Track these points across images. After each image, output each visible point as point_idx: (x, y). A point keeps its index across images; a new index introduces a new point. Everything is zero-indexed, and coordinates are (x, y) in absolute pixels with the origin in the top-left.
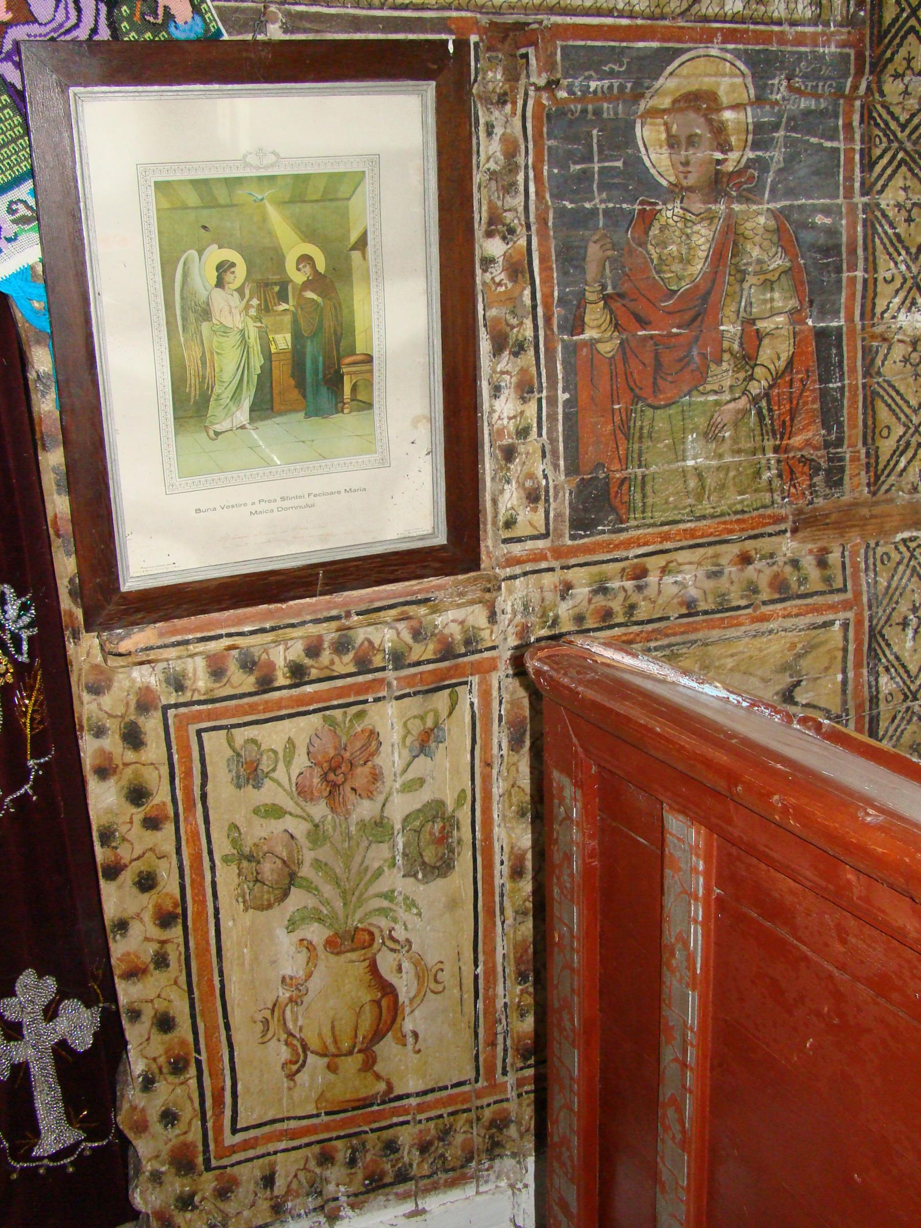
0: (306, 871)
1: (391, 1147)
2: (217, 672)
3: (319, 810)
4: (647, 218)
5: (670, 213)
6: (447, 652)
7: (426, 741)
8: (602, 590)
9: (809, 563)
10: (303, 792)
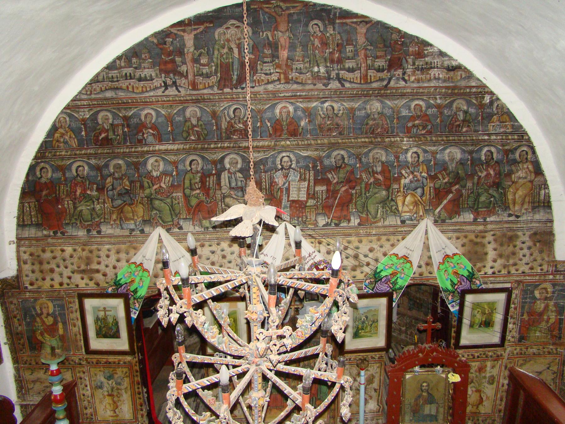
0: (474, 381)
1: (478, 420)
2: (468, 355)
3: (477, 374)
4: (535, 302)
5: (538, 302)
7: (493, 367)
8: (521, 350)
10: (476, 371)
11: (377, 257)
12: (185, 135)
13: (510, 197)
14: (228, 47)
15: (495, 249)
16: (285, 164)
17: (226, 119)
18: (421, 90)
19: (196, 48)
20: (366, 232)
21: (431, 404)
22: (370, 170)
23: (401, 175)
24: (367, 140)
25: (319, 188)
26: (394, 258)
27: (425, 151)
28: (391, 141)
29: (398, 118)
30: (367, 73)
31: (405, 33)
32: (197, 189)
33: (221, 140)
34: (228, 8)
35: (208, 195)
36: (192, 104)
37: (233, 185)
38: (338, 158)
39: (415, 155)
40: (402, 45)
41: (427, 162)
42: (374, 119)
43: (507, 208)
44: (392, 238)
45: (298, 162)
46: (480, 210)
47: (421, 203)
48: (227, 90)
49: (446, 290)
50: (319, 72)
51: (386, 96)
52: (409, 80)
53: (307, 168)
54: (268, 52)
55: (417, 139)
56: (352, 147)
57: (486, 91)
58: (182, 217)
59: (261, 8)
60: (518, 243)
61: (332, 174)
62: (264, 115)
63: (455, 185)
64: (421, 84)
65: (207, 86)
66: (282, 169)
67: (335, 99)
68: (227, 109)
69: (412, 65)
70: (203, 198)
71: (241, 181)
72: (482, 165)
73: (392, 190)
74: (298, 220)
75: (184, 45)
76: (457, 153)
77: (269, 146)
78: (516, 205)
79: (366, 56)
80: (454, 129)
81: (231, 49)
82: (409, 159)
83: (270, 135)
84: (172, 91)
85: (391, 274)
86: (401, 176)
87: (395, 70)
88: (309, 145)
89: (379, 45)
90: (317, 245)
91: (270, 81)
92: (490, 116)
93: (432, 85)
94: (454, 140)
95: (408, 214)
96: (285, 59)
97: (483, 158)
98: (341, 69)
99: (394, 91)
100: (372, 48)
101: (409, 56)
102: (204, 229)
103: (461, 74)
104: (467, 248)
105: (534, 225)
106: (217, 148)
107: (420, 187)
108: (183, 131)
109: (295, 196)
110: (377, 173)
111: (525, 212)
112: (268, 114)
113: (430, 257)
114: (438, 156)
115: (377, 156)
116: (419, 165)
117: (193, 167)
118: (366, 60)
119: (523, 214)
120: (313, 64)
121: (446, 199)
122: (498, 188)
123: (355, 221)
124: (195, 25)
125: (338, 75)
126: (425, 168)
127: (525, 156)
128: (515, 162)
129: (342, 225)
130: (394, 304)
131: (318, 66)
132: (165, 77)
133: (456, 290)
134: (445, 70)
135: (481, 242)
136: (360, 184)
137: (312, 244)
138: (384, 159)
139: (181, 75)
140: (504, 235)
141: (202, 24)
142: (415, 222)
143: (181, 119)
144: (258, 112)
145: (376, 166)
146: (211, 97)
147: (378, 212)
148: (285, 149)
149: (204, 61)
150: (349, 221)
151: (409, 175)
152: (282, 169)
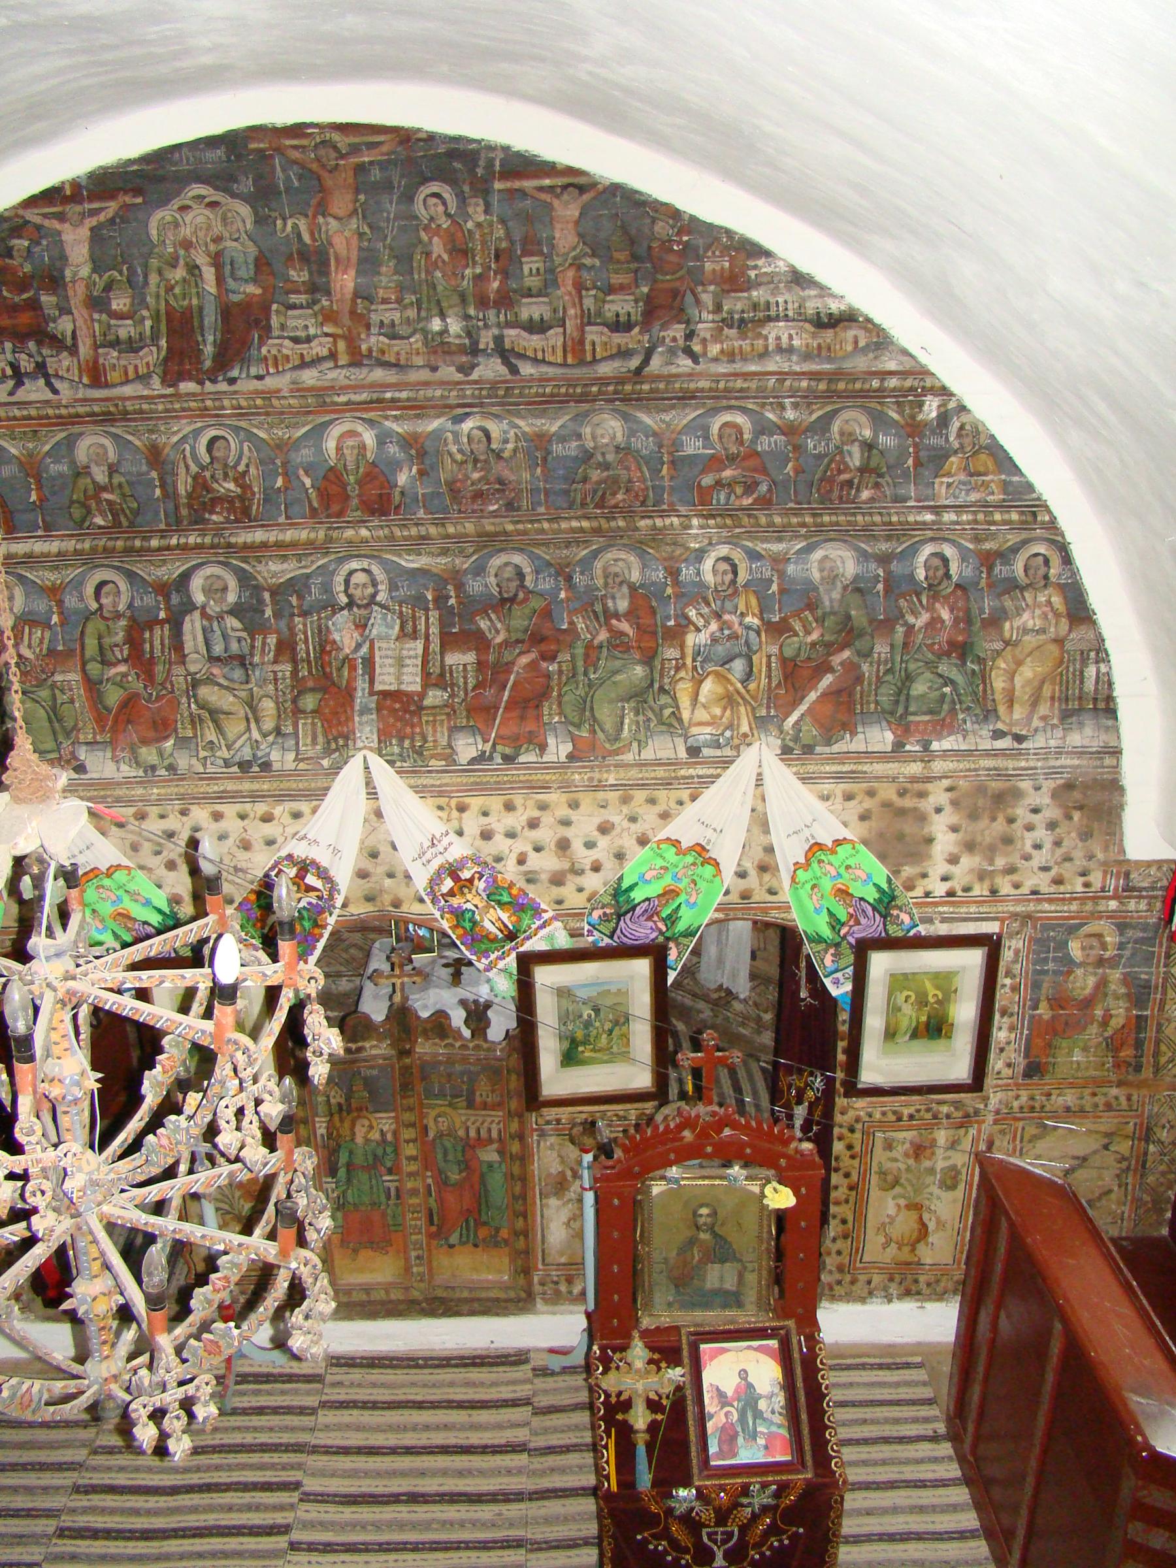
0: (902, 1181)
1: (916, 1281)
2: (884, 1114)
3: (911, 1162)
4: (1069, 973)
5: (1079, 972)
6: (967, 1116)
8: (1032, 1098)
9: (1123, 1100)
10: (906, 1155)
11: (622, 847)
12: (77, 512)
13: (999, 683)
14: (187, 264)
15: (954, 829)
16: (357, 593)
17: (187, 467)
18: (739, 384)
19: (98, 266)
20: (591, 779)
21: (723, 1261)
22: (598, 608)
23: (684, 622)
24: (585, 524)
25: (454, 659)
26: (670, 853)
27: (753, 556)
28: (654, 527)
29: (672, 462)
30: (583, 332)
31: (693, 219)
32: (119, 662)
33: (176, 524)
34: (185, 150)
35: (150, 677)
36: (91, 427)
37: (218, 649)
38: (506, 575)
39: (724, 566)
40: (682, 254)
41: (758, 587)
42: (606, 466)
43: (989, 713)
44: (661, 795)
45: (393, 587)
46: (911, 718)
47: (743, 698)
48: (187, 386)
49: (819, 940)
50: (444, 331)
51: (637, 400)
52: (705, 354)
53: (418, 602)
54: (299, 275)
55: (729, 522)
56: (546, 544)
57: (928, 384)
58: (81, 737)
59: (279, 150)
60: (1021, 812)
61: (490, 619)
62: (293, 455)
63: (841, 649)
64: (738, 367)
65: (131, 375)
66: (351, 605)
67: (495, 410)
68: (189, 440)
69: (714, 312)
70: (137, 685)
71: (239, 640)
72: (918, 595)
73: (663, 664)
74: (400, 744)
75: (64, 258)
76: (843, 560)
77: (310, 543)
78: (1016, 706)
79: (579, 287)
80: (836, 494)
81: (193, 269)
82: (709, 578)
83: (314, 512)
84: (35, 391)
85: (659, 896)
86: (685, 624)
87: (664, 327)
88: (423, 538)
89: (616, 255)
90: (455, 814)
91: (308, 359)
92: (939, 458)
93: (772, 367)
94: (837, 524)
95: (708, 730)
96: (349, 296)
97: (921, 574)
98: (509, 325)
99: (662, 386)
100: (597, 263)
101: (703, 285)
102: (145, 772)
103: (856, 337)
104: (873, 824)
105: (1064, 761)
106: (168, 548)
107: (739, 655)
108: (72, 502)
109: (391, 679)
110: (617, 616)
111: (1042, 724)
112: (305, 454)
113: (770, 850)
114: (791, 569)
115: (617, 570)
116: (736, 593)
117: (104, 601)
118: (581, 298)
119: (1036, 730)
120: (429, 310)
121: (814, 687)
122: (963, 657)
123: (558, 749)
124: (90, 201)
125: (498, 340)
126: (754, 601)
127: (1043, 570)
128: (1012, 586)
129: (522, 759)
130: (672, 976)
131: (443, 316)
132: (14, 352)
133: (844, 938)
134: (807, 326)
135: (915, 809)
136: (571, 646)
137: (440, 813)
138: (635, 576)
139: (57, 342)
140: (981, 790)
141: (112, 196)
142: (727, 752)
143: (64, 468)
144: (278, 447)
145: (613, 598)
146: (145, 407)
147: (622, 723)
148: (355, 550)
149: (119, 303)
150: (543, 747)
151: (707, 623)
152: (351, 605)
